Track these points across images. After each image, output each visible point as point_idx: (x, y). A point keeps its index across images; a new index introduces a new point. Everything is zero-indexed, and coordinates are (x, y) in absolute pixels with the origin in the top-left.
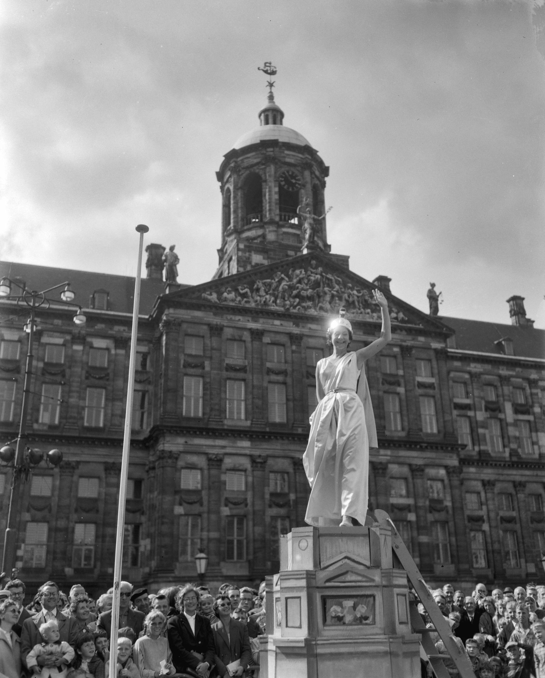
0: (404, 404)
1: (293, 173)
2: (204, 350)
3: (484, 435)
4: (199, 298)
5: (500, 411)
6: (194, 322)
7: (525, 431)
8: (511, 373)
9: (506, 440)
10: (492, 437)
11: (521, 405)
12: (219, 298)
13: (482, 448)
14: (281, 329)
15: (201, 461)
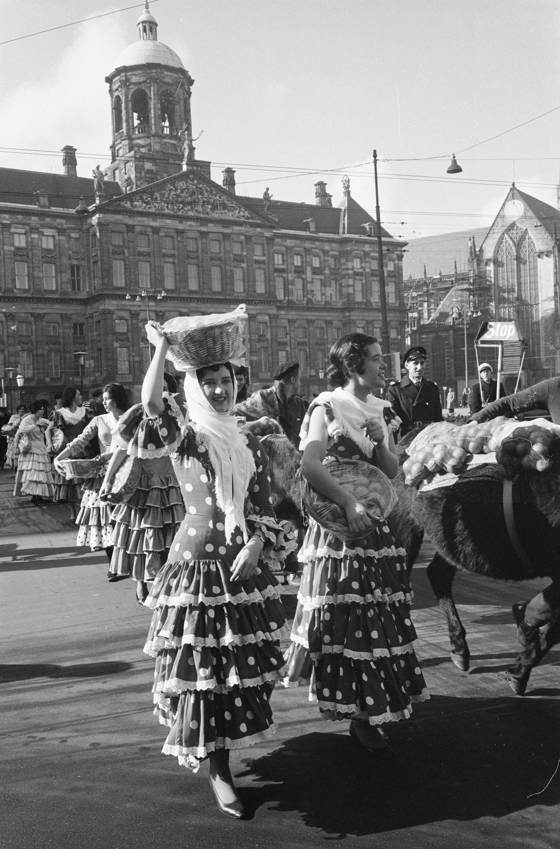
0: (246, 275)
1: (171, 91)
2: (124, 242)
4: (119, 205)
5: (303, 273)
6: (116, 223)
7: (317, 286)
8: (312, 246)
9: (305, 293)
11: (317, 268)
12: (132, 205)
13: (290, 298)
15: (126, 315)
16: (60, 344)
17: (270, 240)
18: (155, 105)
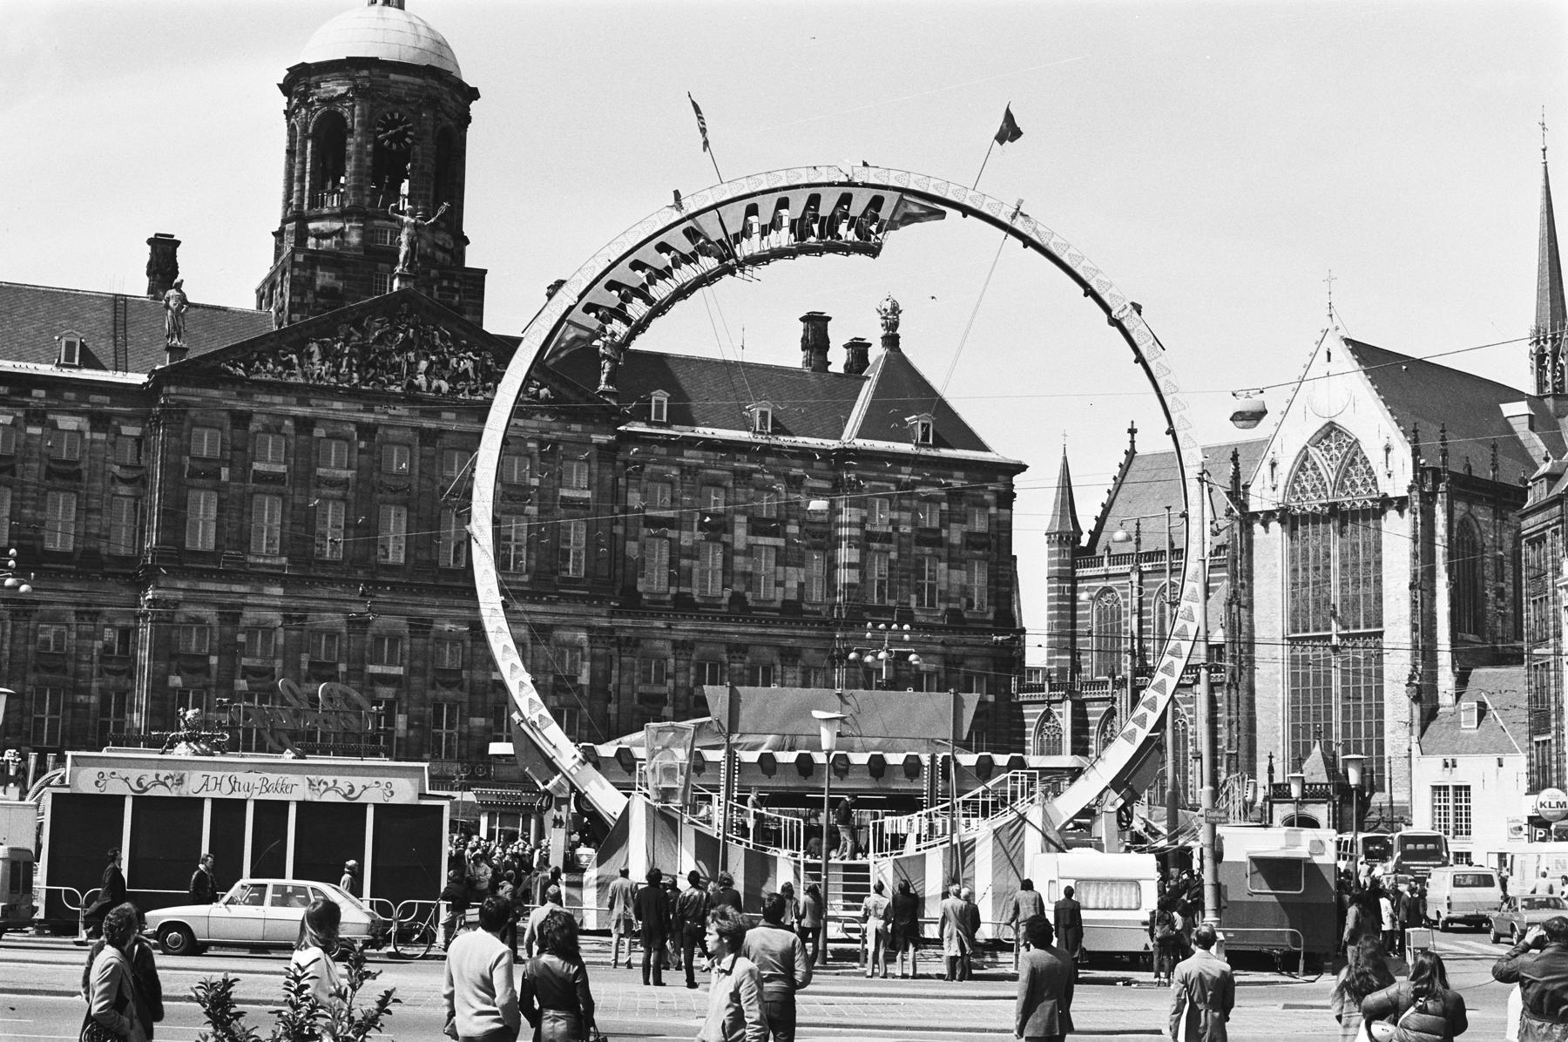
3: (690, 570)
10: (703, 573)
13: (682, 589)
14: (343, 416)
15: (210, 614)
16: (65, 671)
17: (607, 454)
18: (360, 146)
